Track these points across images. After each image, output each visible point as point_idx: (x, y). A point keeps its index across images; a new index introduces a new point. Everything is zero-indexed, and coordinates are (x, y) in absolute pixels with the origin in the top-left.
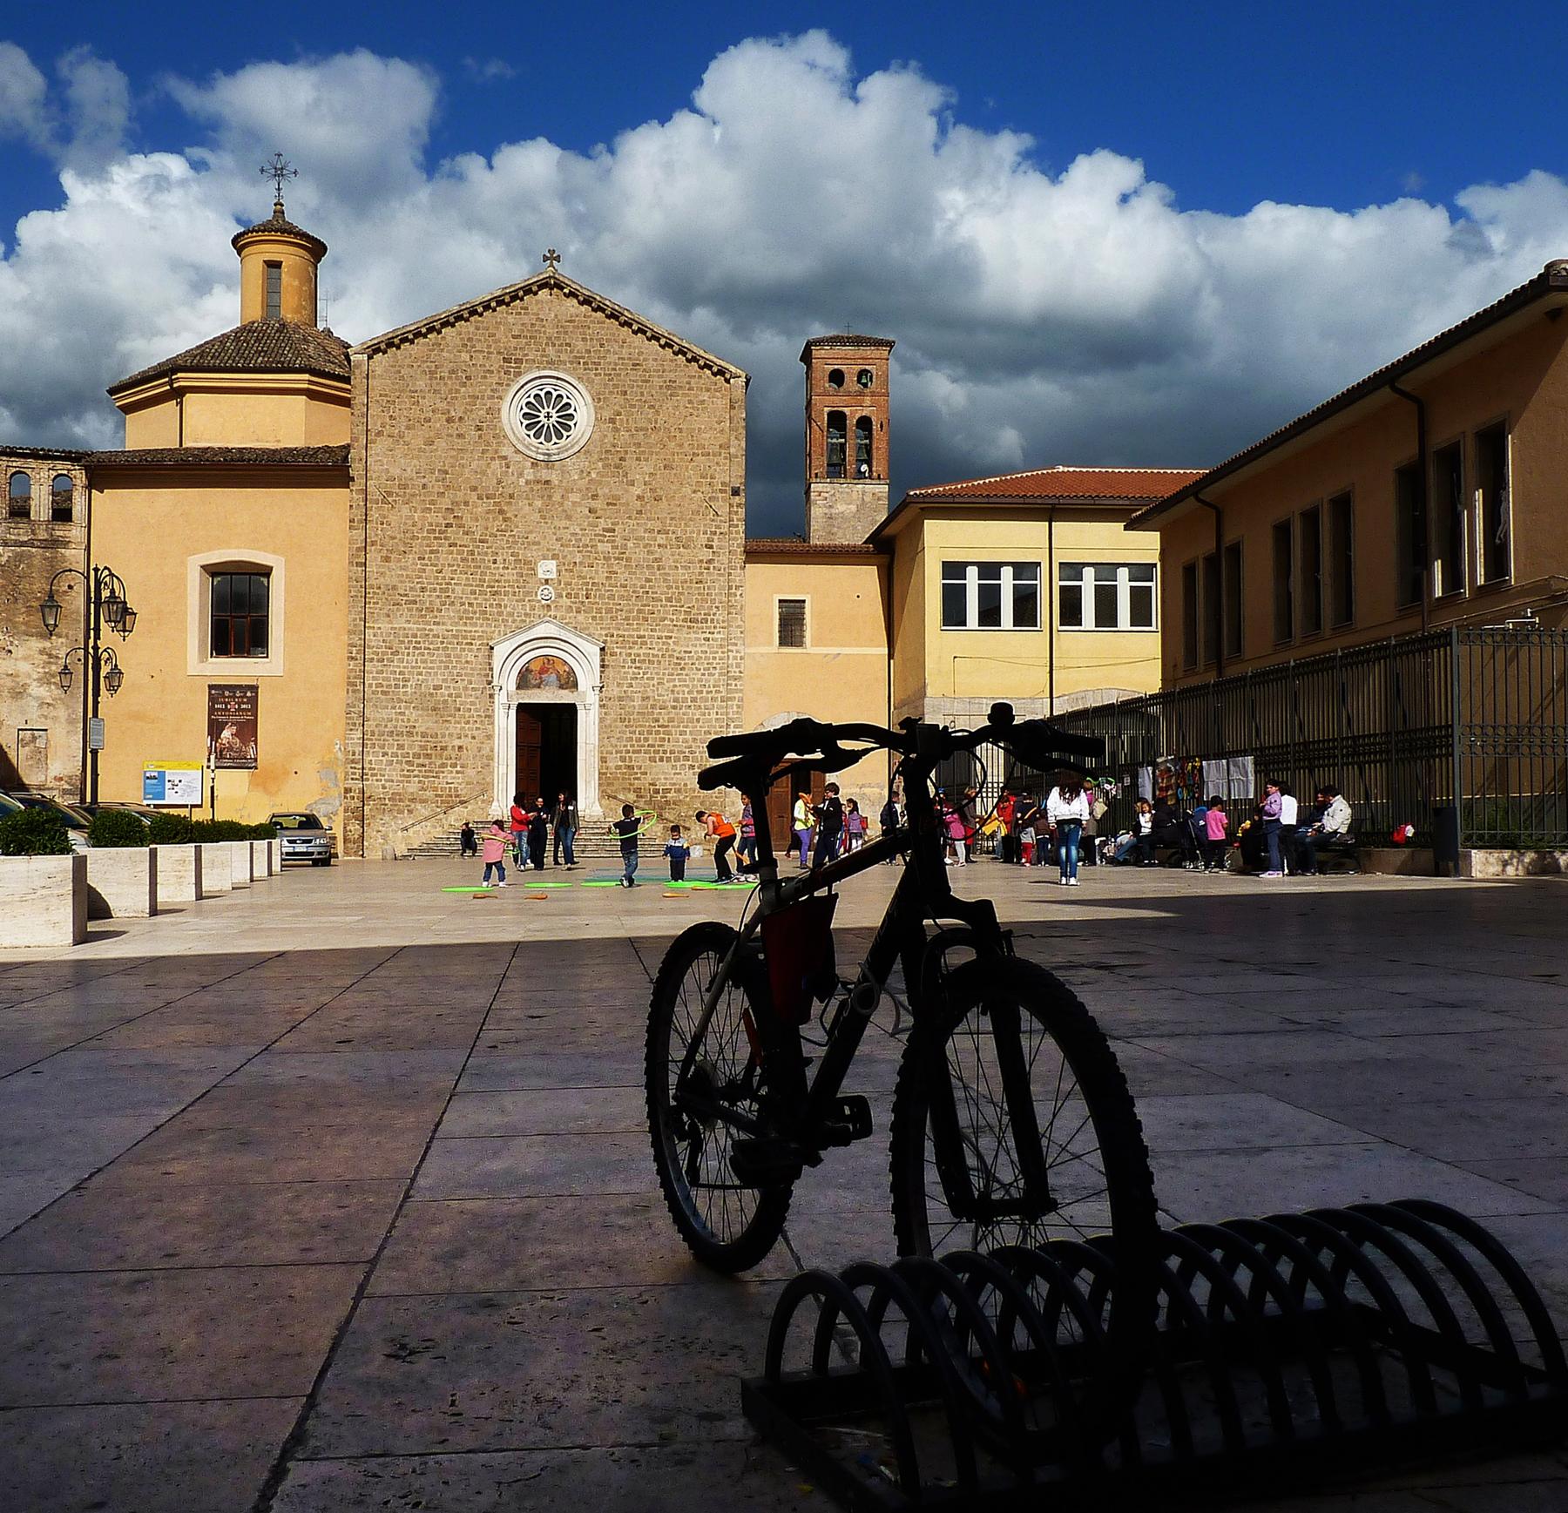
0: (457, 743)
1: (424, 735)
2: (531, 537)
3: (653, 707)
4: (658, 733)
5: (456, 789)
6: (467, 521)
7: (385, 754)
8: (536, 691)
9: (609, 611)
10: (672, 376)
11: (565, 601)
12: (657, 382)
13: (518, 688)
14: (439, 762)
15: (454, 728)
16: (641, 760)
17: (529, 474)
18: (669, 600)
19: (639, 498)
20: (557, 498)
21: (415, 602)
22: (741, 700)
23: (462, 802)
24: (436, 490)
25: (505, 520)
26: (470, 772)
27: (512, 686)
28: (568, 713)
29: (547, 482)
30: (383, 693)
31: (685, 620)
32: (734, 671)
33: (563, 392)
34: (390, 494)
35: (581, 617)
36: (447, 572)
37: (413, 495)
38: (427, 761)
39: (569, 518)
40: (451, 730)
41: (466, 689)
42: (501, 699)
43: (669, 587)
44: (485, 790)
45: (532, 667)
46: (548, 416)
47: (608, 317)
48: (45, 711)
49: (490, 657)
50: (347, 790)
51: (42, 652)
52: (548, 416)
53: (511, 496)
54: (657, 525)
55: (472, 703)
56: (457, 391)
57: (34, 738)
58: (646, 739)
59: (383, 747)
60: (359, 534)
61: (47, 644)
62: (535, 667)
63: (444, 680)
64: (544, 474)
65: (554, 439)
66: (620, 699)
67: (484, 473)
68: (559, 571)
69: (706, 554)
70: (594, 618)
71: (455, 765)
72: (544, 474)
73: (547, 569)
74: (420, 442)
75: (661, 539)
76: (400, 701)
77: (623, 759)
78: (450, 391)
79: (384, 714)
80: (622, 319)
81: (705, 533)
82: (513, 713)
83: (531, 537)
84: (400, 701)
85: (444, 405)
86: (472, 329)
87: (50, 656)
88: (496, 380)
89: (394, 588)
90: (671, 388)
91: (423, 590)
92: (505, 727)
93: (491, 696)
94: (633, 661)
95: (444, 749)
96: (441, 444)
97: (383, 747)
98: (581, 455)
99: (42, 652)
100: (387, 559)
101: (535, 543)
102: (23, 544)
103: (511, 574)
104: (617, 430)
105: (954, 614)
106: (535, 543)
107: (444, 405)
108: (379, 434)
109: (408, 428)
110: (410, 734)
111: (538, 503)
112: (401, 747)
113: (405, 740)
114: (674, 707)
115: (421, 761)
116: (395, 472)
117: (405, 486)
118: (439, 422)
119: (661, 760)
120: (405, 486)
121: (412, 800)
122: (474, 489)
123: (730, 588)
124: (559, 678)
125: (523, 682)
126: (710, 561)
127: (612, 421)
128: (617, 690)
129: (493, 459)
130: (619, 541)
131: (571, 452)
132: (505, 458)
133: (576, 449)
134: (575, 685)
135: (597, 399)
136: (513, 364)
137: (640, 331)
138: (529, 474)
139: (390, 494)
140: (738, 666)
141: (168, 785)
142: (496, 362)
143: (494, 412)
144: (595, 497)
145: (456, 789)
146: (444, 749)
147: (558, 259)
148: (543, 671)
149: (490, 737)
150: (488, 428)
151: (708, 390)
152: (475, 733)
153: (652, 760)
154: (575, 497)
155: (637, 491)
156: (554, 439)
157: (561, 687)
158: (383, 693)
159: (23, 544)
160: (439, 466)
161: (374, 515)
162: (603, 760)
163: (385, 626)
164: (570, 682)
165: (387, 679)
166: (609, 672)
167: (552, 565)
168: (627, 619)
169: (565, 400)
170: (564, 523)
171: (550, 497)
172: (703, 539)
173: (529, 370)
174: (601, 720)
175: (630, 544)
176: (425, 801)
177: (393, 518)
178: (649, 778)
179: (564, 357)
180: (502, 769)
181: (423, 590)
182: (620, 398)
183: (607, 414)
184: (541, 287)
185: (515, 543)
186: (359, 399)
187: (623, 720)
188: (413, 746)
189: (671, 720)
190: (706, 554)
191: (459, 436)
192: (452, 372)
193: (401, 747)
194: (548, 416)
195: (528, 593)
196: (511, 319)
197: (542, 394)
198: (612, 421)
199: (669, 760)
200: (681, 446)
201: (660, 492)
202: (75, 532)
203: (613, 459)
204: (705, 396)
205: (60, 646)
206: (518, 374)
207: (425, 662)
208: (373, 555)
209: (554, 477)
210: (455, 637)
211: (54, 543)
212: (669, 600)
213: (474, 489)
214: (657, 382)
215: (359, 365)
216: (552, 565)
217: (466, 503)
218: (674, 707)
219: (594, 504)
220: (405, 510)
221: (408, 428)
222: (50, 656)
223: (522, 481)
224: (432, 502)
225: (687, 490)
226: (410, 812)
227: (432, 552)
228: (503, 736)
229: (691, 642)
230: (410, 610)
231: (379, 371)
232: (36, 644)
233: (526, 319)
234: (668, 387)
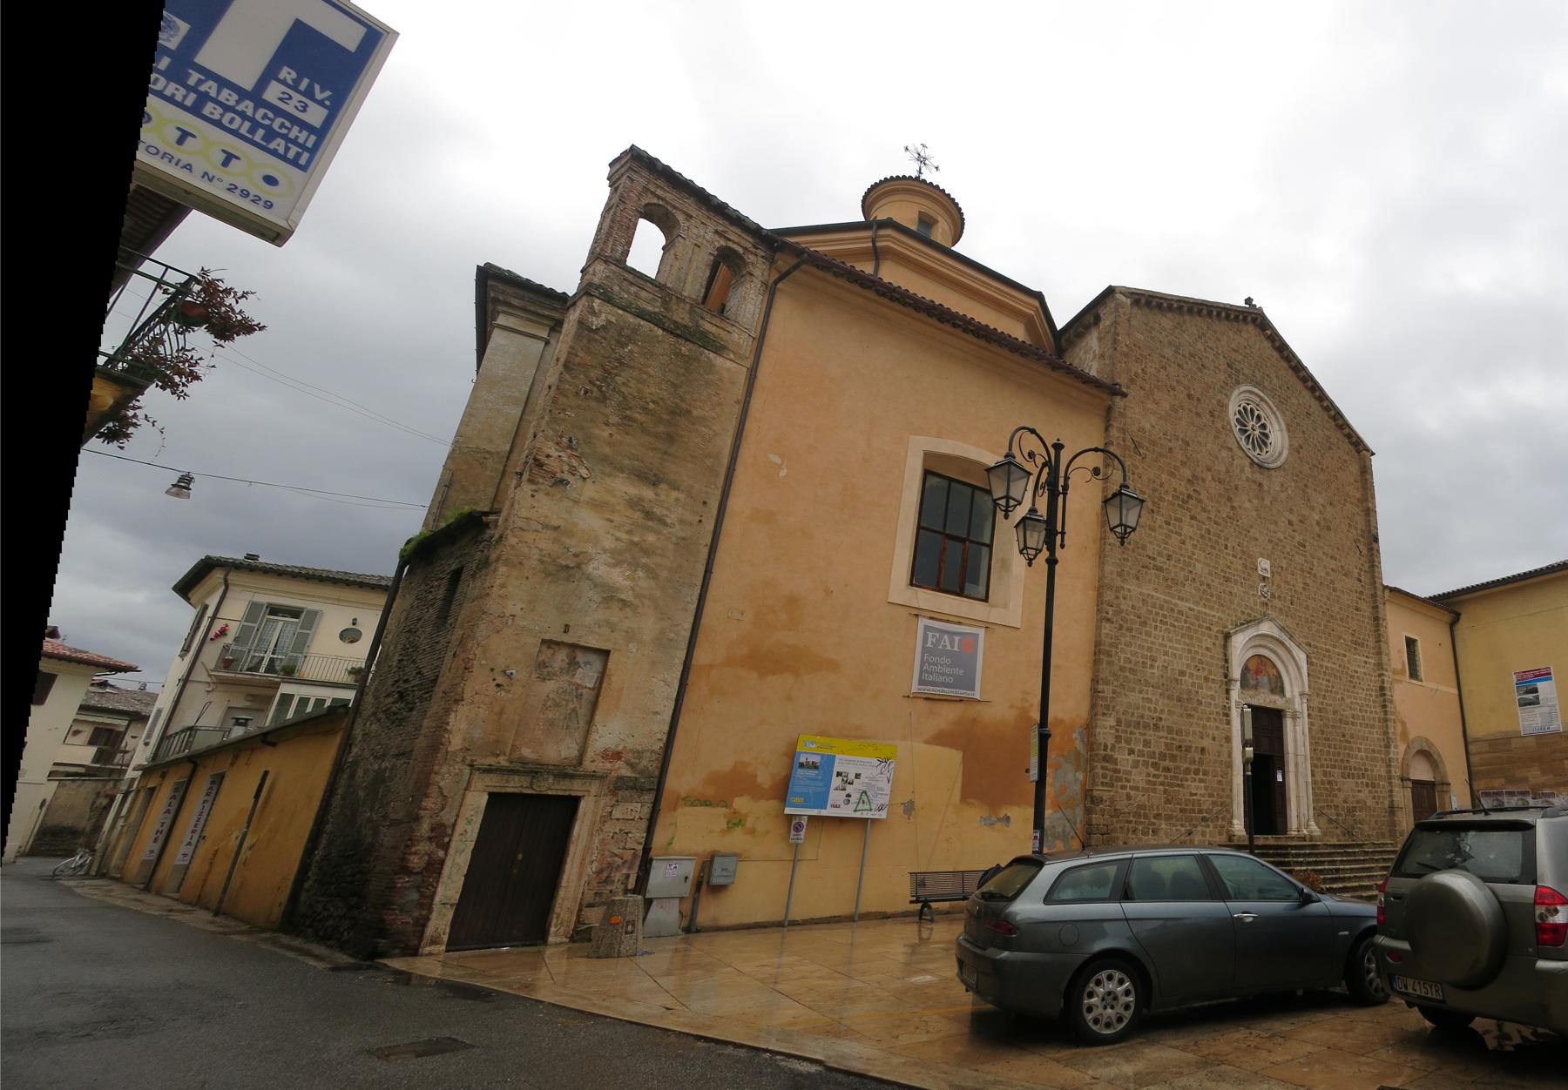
1: (1170, 730)
7: (1131, 752)
36: (1189, 546)
45: (1252, 666)
49: (1225, 647)
55: (1213, 697)
59: (1128, 742)
62: (1252, 666)
71: (1197, 772)
73: (1264, 564)
76: (1147, 684)
79: (1135, 698)
84: (1147, 684)
91: (1169, 557)
95: (1188, 749)
97: (1128, 742)
112: (1147, 743)
113: (1151, 735)
115: (1167, 763)
121: (1158, 816)
134: (1282, 691)
146: (1188, 749)
157: (1272, 691)
158: (1132, 671)
164: (1278, 689)
176: (1169, 818)
193: (1147, 743)
210: (1197, 618)
230: (1157, 577)
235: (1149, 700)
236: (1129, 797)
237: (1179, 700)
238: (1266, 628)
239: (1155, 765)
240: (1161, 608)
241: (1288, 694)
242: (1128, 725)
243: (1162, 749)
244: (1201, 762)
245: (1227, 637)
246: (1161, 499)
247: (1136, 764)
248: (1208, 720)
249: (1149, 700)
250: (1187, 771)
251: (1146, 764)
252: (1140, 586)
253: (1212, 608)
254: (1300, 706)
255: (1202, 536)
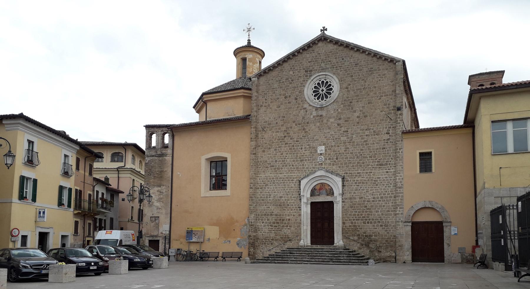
0: (288, 218)
1: (276, 215)
2: (315, 138)
3: (364, 201)
4: (366, 212)
5: (288, 235)
6: (291, 134)
7: (263, 223)
8: (318, 197)
9: (346, 164)
10: (371, 66)
11: (328, 161)
12: (365, 69)
13: (311, 196)
14: (282, 225)
15: (287, 212)
16: (359, 223)
17: (314, 113)
18: (371, 157)
19: (358, 117)
20: (325, 121)
21: (273, 166)
22: (402, 196)
23: (290, 240)
24: (280, 124)
25: (305, 132)
26: (292, 228)
27: (309, 196)
28: (331, 204)
29: (321, 116)
30: (263, 200)
31: (377, 165)
32: (399, 184)
33: (328, 80)
34: (265, 127)
35: (334, 167)
36: (284, 155)
37: (273, 127)
38: (277, 225)
39: (329, 128)
40: (286, 213)
41: (291, 197)
42: (304, 200)
43: (370, 152)
44: (298, 236)
46: (323, 90)
47: (345, 47)
48: (159, 210)
49: (300, 185)
50: (250, 236)
51: (158, 191)
52: (323, 90)
53: (308, 123)
54: (366, 127)
56: (288, 86)
57: (155, 220)
58: (362, 215)
60: (253, 143)
61: (160, 189)
62: (318, 188)
63: (284, 194)
64: (320, 113)
65: (325, 99)
66: (351, 199)
67: (298, 115)
68: (326, 150)
69: (387, 137)
70: (340, 167)
71: (287, 226)
72: (320, 113)
73: (321, 149)
74: (275, 107)
75: (367, 133)
77: (352, 223)
78: (286, 87)
79: (263, 208)
80: (350, 47)
81: (386, 128)
82: (309, 206)
83: (315, 138)
85: (284, 92)
86: (294, 62)
87: (160, 192)
88: (302, 79)
89: (266, 161)
90: (371, 71)
91: (276, 161)
92: (306, 210)
93: (300, 200)
94: (356, 183)
95: (283, 220)
96: (283, 107)
98: (335, 103)
99: (158, 191)
100: (264, 151)
101: (318, 140)
102: (153, 156)
103: (307, 153)
104: (349, 91)
105: (22, 197)
106: (318, 140)
107: (284, 92)
108: (262, 106)
109: (271, 102)
110: (271, 215)
111: (318, 124)
112: (268, 220)
114: (373, 201)
115: (275, 225)
116: (267, 119)
117: (269, 124)
118: (282, 98)
119: (368, 223)
120: (269, 124)
122: (294, 122)
123: (397, 149)
124: (326, 191)
125: (313, 194)
126: (388, 139)
127: (347, 88)
128: (349, 195)
129: (301, 109)
130: (350, 135)
131: (330, 103)
132: (305, 108)
133: (332, 101)
134: (333, 194)
135: (341, 80)
136: (309, 72)
137: (358, 50)
138: (314, 113)
139: (265, 127)
140: (401, 182)
141: (193, 235)
142: (303, 72)
143: (302, 92)
144: (340, 119)
145: (288, 235)
146: (283, 220)
147: (326, 30)
148: (320, 189)
149: (300, 215)
150: (300, 98)
151: (387, 69)
152: (295, 214)
153: (364, 223)
154: (332, 120)
155: (357, 114)
156: (325, 99)
157: (328, 195)
158: (263, 200)
159: (153, 156)
160: (282, 115)
161: (260, 136)
162: (344, 223)
163: (263, 176)
164: (331, 192)
165: (264, 195)
166: (346, 188)
167: (323, 148)
168: (353, 166)
169: (329, 83)
170: (328, 131)
171: (322, 121)
172: (385, 131)
173: (315, 74)
174: (343, 207)
175: (354, 136)
176: (276, 240)
177: (266, 136)
178: (363, 230)
179: (328, 66)
180: (305, 227)
181: (276, 161)
182: (350, 79)
183: (345, 86)
184: (318, 41)
185: (309, 140)
186: (254, 94)
187: (351, 207)
188: (272, 219)
189: (372, 206)
190: (387, 137)
191: (289, 103)
192: (287, 79)
193: (268, 220)
194: (323, 90)
195: (314, 159)
196: (308, 56)
197: (320, 82)
198: (347, 88)
199: (371, 223)
200: (375, 93)
201: (366, 114)
202: (169, 151)
203: (347, 103)
204: (386, 72)
205: (164, 189)
206: (311, 76)
207: (276, 188)
208: (260, 150)
209: (324, 113)
211: (162, 155)
212: (371, 157)
213: (294, 122)
214: (365, 69)
215: (254, 82)
216: (323, 148)
217: (291, 128)
218: (373, 201)
219: (339, 122)
220: (270, 133)
221: (271, 102)
222: (160, 192)
223: (312, 116)
224: (280, 129)
225: (378, 111)
226: (272, 244)
227: (279, 147)
228: (305, 215)
229: (381, 174)
230: (271, 169)
231: (261, 83)
232: (156, 189)
233: (314, 55)
234: (370, 71)
235: (269, 207)
236: (263, 235)
237: (280, 205)
238: (319, 173)
239: (271, 226)
240: (273, 179)
241: (335, 195)
242: (262, 215)
243: (274, 221)
244: (288, 223)
245: (300, 182)
246: (273, 142)
247: (265, 226)
248: (292, 210)
249: (269, 207)
250: (283, 226)
251: (268, 225)
252: (265, 174)
253: (294, 173)
254: (339, 199)
255: (290, 149)
